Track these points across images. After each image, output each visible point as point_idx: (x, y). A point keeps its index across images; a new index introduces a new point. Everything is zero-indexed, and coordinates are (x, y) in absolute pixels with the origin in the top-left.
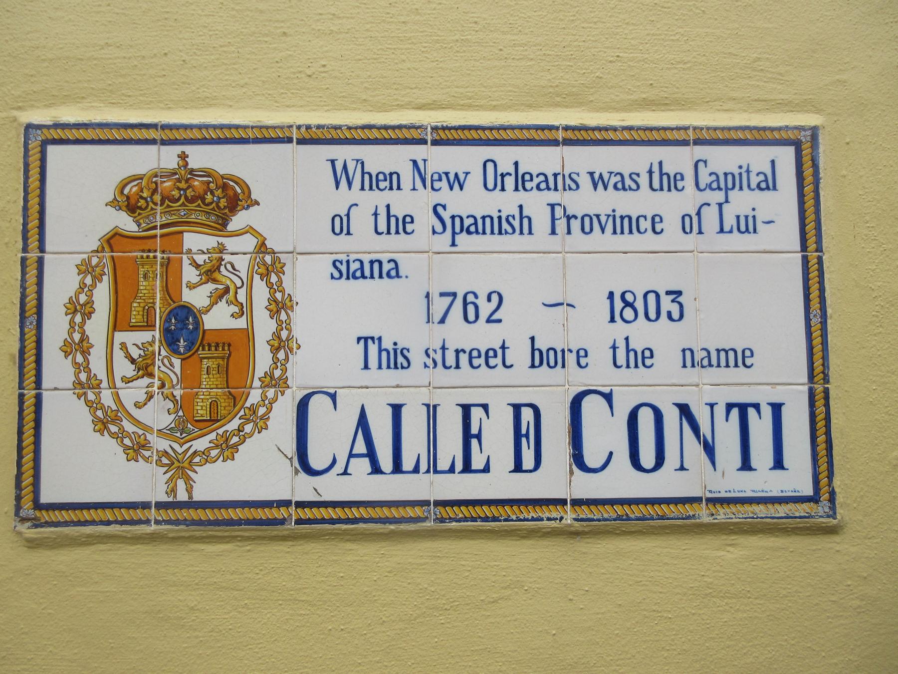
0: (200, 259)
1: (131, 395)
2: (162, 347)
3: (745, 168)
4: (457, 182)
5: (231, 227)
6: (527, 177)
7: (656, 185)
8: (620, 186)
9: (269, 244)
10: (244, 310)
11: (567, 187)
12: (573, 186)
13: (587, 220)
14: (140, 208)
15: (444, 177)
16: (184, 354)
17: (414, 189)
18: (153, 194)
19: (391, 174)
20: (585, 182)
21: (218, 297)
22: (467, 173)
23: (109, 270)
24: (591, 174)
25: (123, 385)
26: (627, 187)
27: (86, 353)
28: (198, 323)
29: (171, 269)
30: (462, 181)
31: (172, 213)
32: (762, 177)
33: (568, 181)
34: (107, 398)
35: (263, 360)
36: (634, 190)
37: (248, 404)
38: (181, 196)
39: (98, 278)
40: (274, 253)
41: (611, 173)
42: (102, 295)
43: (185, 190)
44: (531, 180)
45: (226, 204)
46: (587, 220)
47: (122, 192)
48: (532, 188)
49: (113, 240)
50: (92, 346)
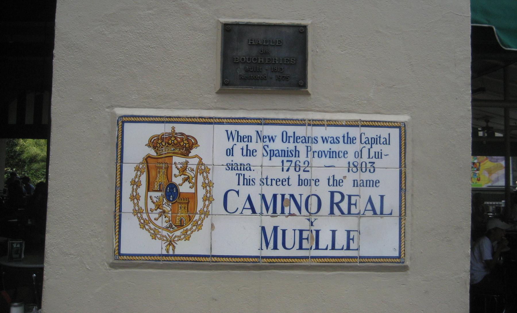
0: (179, 166)
1: (153, 216)
2: (164, 198)
3: (379, 136)
4: (272, 139)
5: (190, 155)
6: (298, 138)
7: (346, 141)
8: (332, 142)
9: (204, 161)
10: (195, 185)
11: (313, 142)
12: (316, 142)
13: (320, 153)
14: (158, 147)
15: (267, 137)
16: (172, 201)
17: (257, 142)
18: (162, 142)
19: (248, 136)
20: (320, 140)
21: (185, 180)
22: (276, 136)
23: (146, 170)
24: (322, 137)
25: (150, 212)
26: (335, 142)
27: (138, 199)
28: (177, 190)
29: (168, 169)
30: (274, 139)
31: (169, 149)
32: (385, 140)
33: (313, 140)
34: (145, 216)
35: (200, 205)
36: (338, 143)
37: (194, 220)
38: (172, 142)
39: (142, 173)
40: (205, 165)
41: (329, 137)
42: (143, 178)
43: (174, 141)
44: (300, 138)
45: (188, 146)
46: (320, 153)
47: (151, 142)
48: (300, 142)
49: (148, 158)
50: (140, 197)
